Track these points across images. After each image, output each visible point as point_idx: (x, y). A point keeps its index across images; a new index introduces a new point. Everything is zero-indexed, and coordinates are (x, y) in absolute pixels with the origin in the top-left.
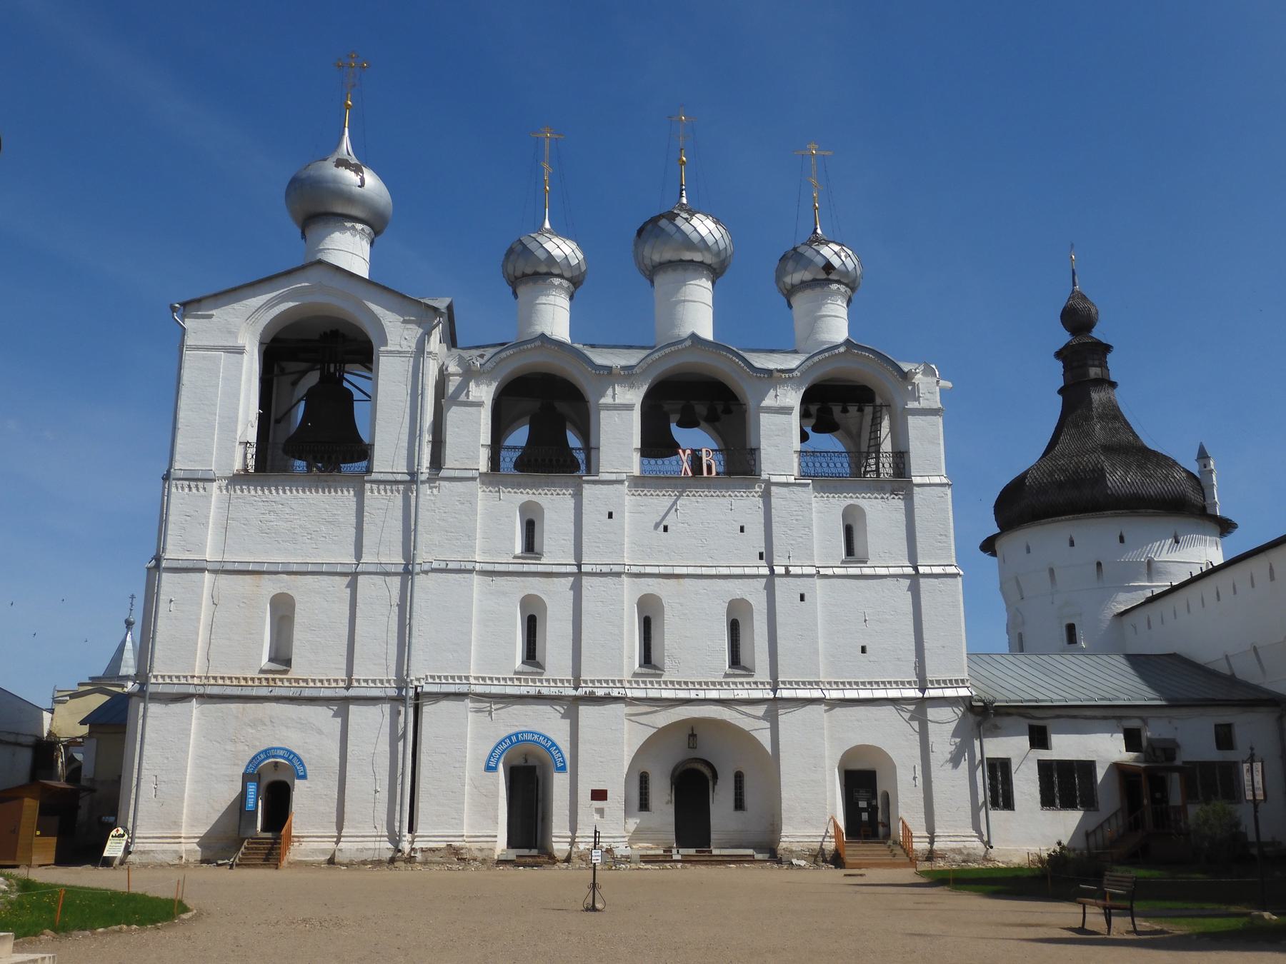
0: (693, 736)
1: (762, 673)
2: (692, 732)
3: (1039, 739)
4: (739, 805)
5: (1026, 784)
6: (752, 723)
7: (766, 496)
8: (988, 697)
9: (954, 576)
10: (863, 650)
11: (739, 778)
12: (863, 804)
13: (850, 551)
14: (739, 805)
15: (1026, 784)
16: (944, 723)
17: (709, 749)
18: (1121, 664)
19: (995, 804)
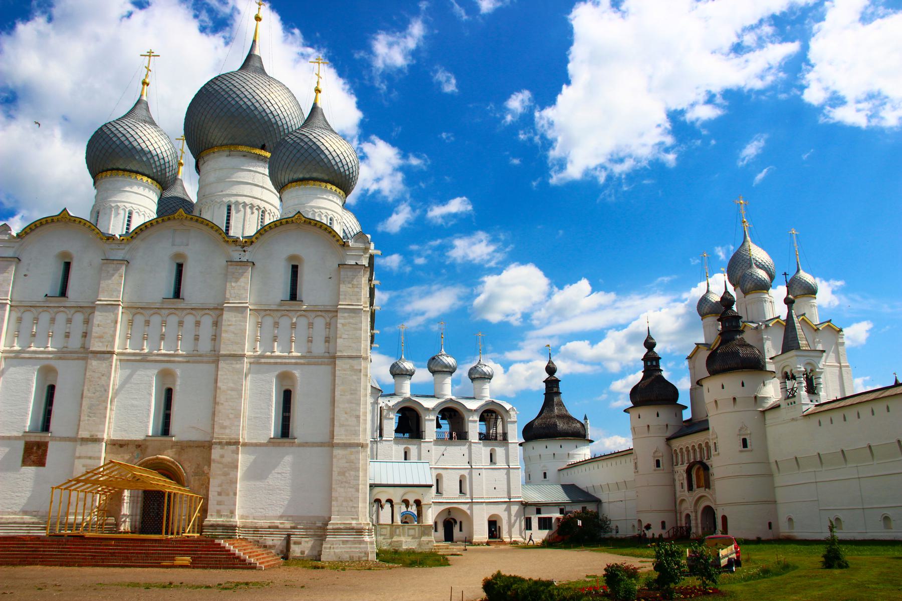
0: (450, 512)
1: (468, 496)
2: (449, 511)
3: (539, 511)
4: (461, 530)
5: (535, 523)
6: (465, 507)
7: (470, 446)
8: (526, 501)
9: (519, 468)
10: (495, 488)
11: (461, 523)
12: (493, 529)
13: (491, 461)
14: (461, 530)
15: (535, 523)
16: (515, 509)
17: (454, 515)
18: (560, 488)
19: (527, 529)
